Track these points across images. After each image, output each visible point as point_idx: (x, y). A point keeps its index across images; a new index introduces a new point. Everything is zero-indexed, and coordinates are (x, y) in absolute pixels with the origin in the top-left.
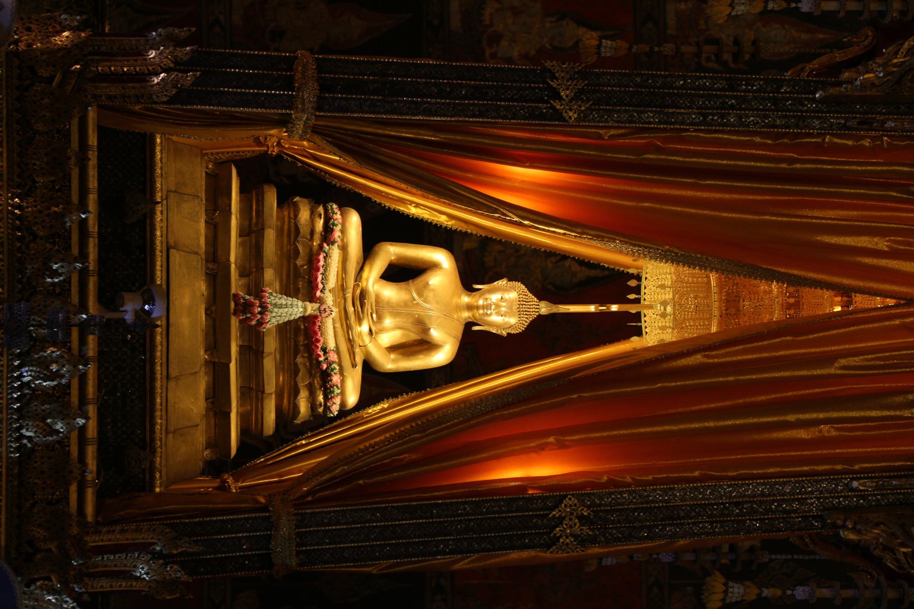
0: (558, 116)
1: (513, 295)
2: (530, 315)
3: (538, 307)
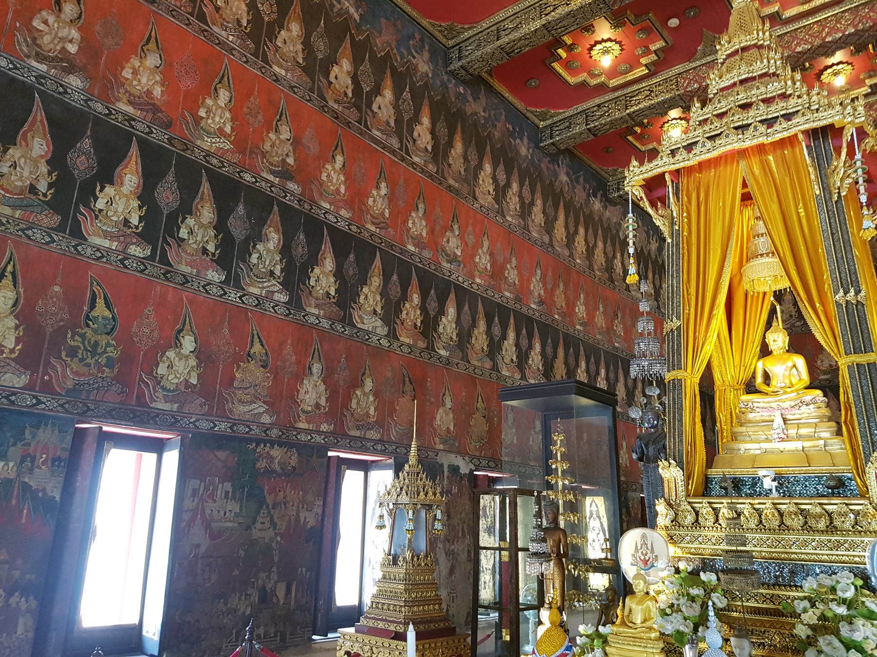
0: (679, 328)
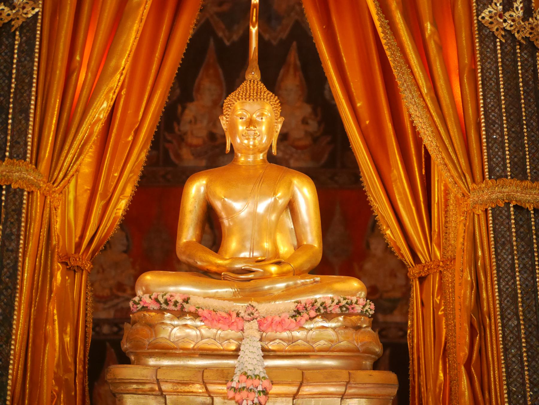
1: (238, 105)
2: (261, 89)
3: (252, 81)
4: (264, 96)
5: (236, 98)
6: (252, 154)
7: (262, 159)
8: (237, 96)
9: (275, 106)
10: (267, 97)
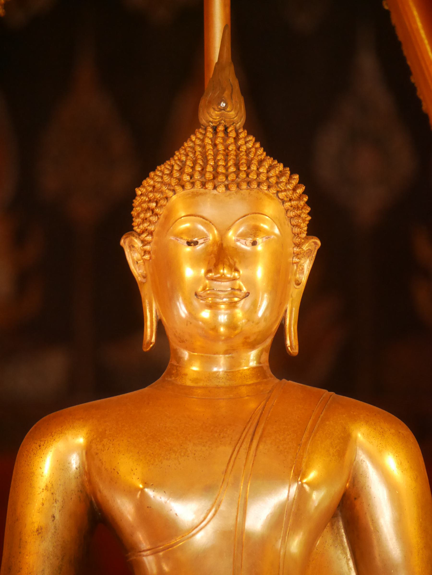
3: (221, 128)
4: (258, 174)
5: (174, 182)
6: (226, 352)
7: (254, 368)
8: (176, 174)
9: (294, 203)
10: (268, 178)
